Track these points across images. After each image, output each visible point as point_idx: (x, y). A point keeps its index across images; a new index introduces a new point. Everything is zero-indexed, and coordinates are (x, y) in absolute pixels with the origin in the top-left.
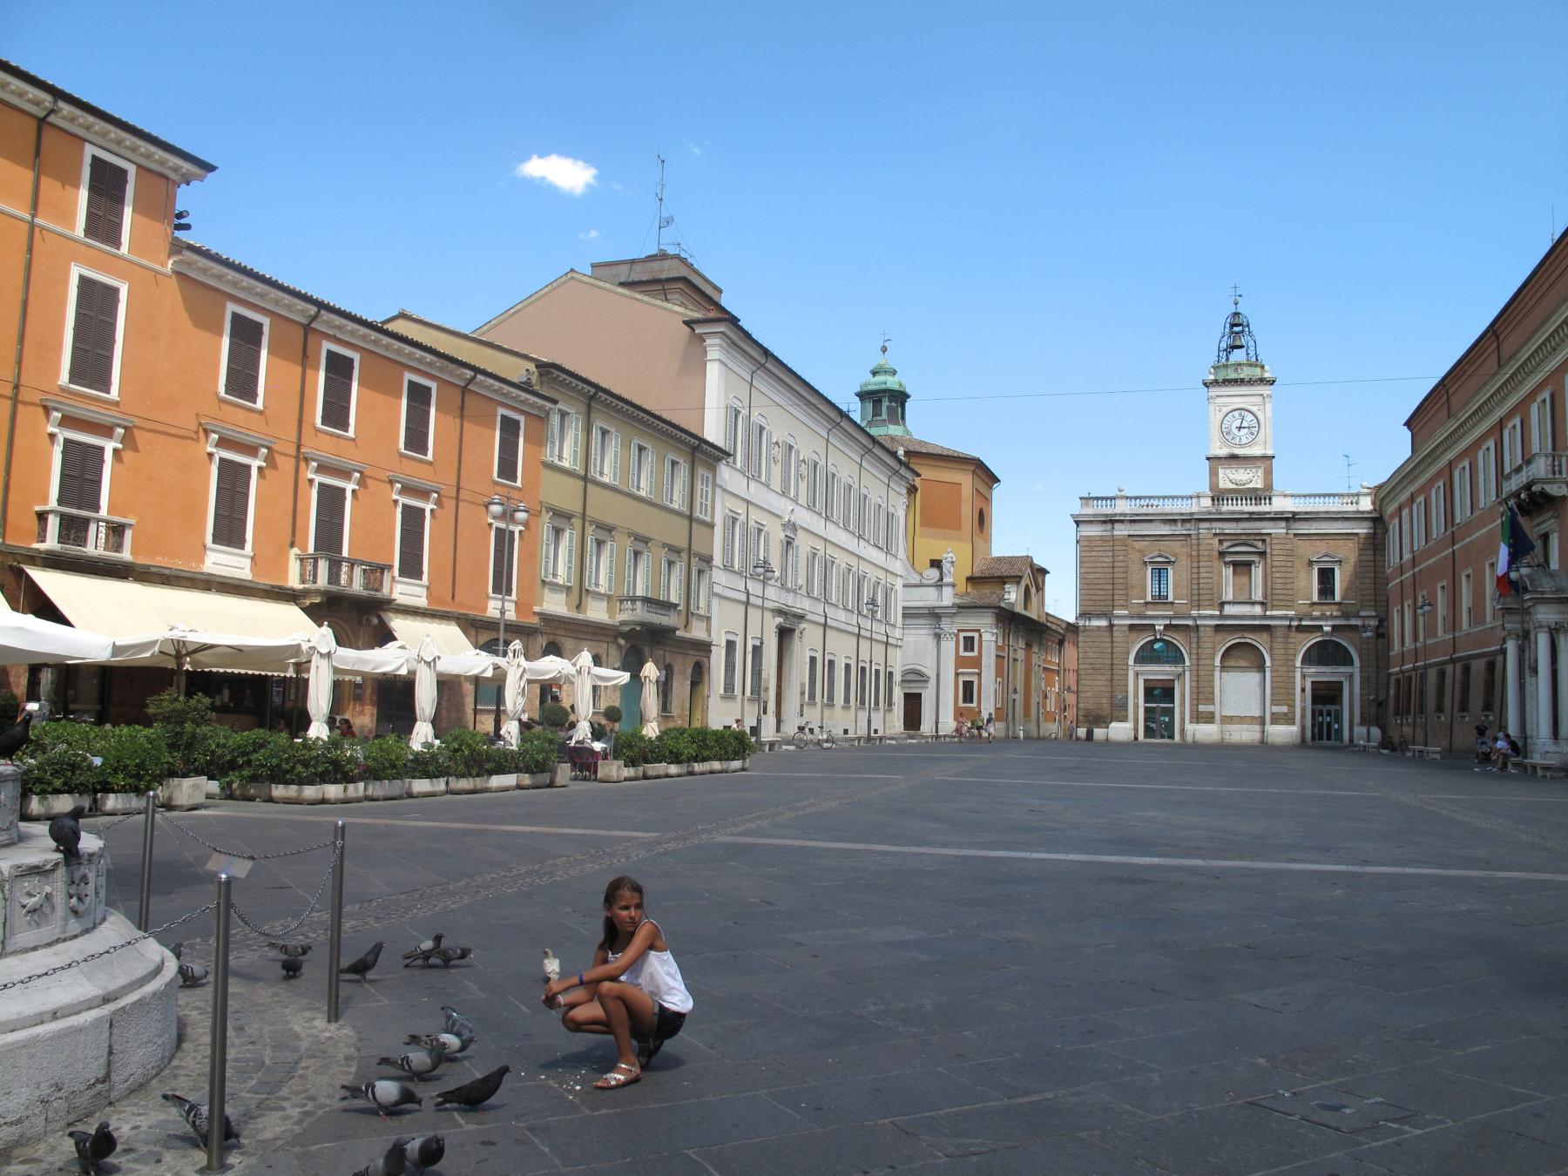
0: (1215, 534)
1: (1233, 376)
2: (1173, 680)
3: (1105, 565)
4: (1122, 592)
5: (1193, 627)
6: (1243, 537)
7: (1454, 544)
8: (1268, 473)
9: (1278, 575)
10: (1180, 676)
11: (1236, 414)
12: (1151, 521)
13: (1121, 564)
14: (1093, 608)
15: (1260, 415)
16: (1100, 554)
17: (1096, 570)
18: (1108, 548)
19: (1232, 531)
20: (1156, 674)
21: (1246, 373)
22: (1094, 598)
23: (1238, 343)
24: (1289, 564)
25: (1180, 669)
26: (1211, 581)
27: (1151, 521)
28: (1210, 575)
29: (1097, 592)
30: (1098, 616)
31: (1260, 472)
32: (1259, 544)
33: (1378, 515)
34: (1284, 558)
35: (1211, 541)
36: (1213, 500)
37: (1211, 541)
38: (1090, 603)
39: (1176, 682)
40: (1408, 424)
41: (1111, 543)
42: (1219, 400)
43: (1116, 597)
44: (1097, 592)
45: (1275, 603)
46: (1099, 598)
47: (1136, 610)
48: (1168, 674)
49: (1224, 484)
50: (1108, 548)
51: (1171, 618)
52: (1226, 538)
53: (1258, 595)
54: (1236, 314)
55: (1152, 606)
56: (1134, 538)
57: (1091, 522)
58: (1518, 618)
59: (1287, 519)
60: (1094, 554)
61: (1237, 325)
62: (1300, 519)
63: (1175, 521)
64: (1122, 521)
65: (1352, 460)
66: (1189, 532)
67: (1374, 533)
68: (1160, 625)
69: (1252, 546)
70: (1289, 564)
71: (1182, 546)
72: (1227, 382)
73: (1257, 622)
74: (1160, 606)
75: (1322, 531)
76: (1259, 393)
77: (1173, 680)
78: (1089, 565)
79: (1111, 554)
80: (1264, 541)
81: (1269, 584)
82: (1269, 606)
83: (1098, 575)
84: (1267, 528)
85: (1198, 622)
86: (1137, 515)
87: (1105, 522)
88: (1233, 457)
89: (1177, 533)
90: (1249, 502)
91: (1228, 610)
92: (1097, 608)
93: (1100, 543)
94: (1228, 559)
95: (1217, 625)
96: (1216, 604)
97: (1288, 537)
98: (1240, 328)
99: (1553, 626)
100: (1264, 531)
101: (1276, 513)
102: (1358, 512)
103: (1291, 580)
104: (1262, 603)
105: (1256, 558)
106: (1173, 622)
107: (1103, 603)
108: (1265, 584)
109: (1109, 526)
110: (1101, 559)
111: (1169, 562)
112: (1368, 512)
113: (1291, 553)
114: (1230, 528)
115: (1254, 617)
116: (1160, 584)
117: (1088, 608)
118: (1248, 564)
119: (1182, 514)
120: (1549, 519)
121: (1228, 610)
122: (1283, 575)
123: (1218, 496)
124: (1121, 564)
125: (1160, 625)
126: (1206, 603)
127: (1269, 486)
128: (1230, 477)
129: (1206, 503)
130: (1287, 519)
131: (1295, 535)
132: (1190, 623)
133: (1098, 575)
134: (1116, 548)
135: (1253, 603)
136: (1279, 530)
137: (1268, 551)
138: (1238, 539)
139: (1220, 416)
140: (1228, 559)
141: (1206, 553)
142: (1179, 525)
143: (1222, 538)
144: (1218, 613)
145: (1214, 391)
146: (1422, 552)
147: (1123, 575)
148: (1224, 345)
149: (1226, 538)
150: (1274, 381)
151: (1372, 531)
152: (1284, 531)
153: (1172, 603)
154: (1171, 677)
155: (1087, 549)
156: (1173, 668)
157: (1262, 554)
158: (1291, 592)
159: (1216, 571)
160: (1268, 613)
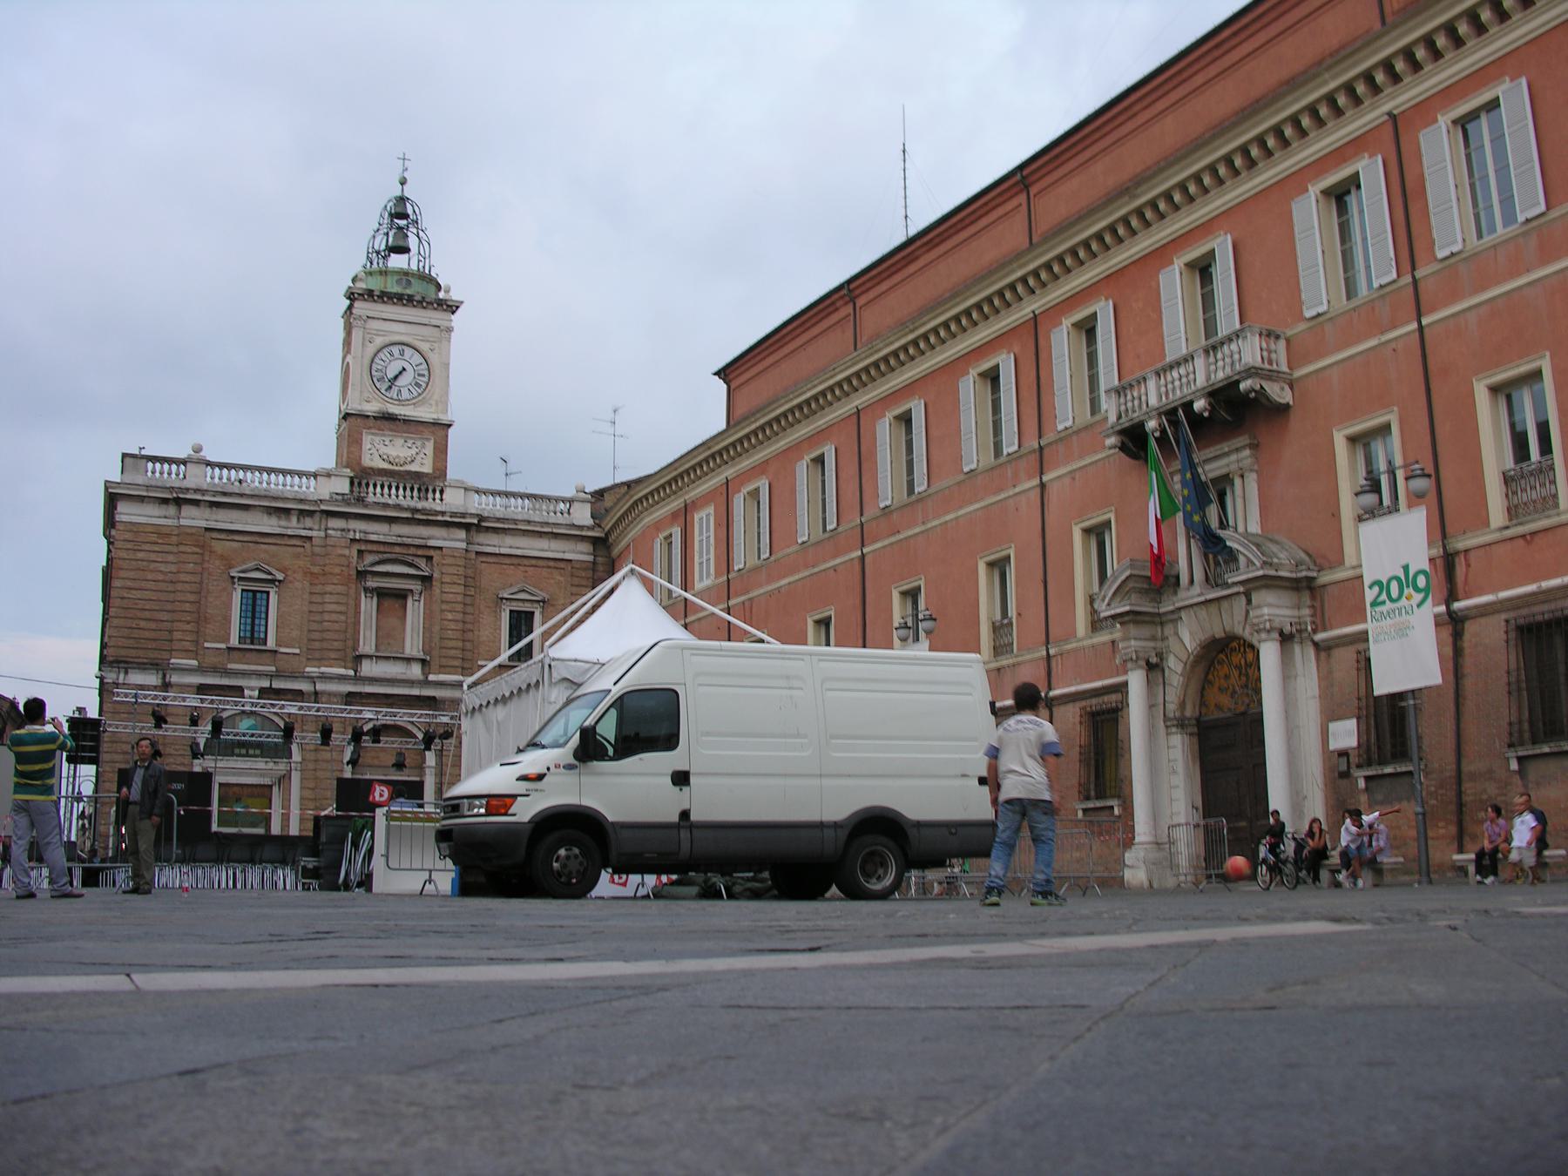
0: (353, 540)
1: (394, 288)
2: (271, 786)
3: (161, 577)
4: (188, 627)
5: (309, 694)
6: (397, 549)
7: (863, 545)
8: (441, 451)
9: (450, 616)
10: (284, 779)
11: (395, 350)
12: (246, 507)
13: (188, 578)
14: (133, 653)
15: (433, 358)
16: (153, 556)
17: (143, 584)
18: (167, 548)
19: (382, 538)
20: (240, 775)
21: (416, 289)
22: (136, 634)
23: (401, 243)
24: (468, 600)
25: (282, 766)
26: (343, 618)
27: (246, 507)
28: (342, 608)
29: (143, 624)
30: (142, 667)
31: (429, 448)
32: (422, 563)
33: (603, 535)
34: (461, 589)
35: (346, 552)
36: (352, 483)
37: (346, 552)
38: (131, 643)
39: (275, 789)
40: (723, 373)
41: (174, 539)
42: (374, 325)
43: (177, 635)
44: (143, 624)
45: (444, 662)
46: (147, 634)
47: (211, 660)
48: (262, 775)
49: (371, 460)
50: (167, 548)
51: (271, 676)
52: (370, 547)
53: (413, 645)
54: (402, 200)
55: (236, 654)
56: (215, 535)
57: (141, 499)
58: (1145, 631)
59: (467, 527)
60: (140, 555)
61: (400, 213)
62: (488, 529)
63: (287, 511)
64: (196, 503)
65: (512, 467)
66: (309, 533)
67: (594, 563)
68: (252, 689)
69: (411, 565)
70: (468, 600)
71: (297, 556)
72: (385, 297)
73: (415, 692)
74: (253, 656)
75: (519, 552)
76: (434, 322)
77: (271, 786)
78: (132, 574)
79: (171, 558)
80: (429, 558)
81: (436, 628)
82: (434, 665)
83: (147, 595)
84: (438, 538)
85: (320, 687)
86: (225, 494)
87: (165, 501)
88: (388, 418)
89: (290, 532)
90: (408, 492)
91: (367, 668)
92: (141, 653)
93: (154, 538)
94: (372, 583)
95: (350, 694)
96: (349, 658)
97: (469, 555)
98: (402, 223)
99: (1287, 629)
100: (432, 543)
101: (453, 514)
102: (573, 526)
103: (469, 626)
104: (423, 662)
105: (416, 586)
106: (277, 684)
107: (153, 645)
108: (427, 629)
109: (172, 510)
110: (152, 566)
111: (272, 581)
112: (589, 528)
113: (470, 581)
114: (378, 532)
115: (411, 683)
116: (253, 618)
117: (123, 652)
118: (401, 596)
119: (301, 501)
120: (1237, 450)
121: (367, 668)
122: (459, 616)
123: (362, 477)
124: (188, 578)
125: (252, 689)
126: (333, 655)
127: (440, 472)
128: (380, 450)
129: (343, 486)
130: (467, 527)
131: (477, 553)
132: (305, 686)
133: (147, 595)
134: (182, 548)
135: (409, 660)
136: (455, 541)
137: (435, 575)
138: (391, 554)
139: (371, 349)
140: (372, 583)
141: (337, 570)
142: (294, 519)
143: (363, 545)
144: (351, 673)
145: (361, 307)
146: (756, 569)
147: (192, 598)
148: (380, 244)
149: (370, 547)
150: (457, 307)
151: (591, 558)
152: (464, 545)
153: (276, 651)
154: (267, 781)
155: (129, 546)
156: (271, 765)
157: (426, 580)
158: (468, 646)
159: (352, 602)
160: (432, 677)
